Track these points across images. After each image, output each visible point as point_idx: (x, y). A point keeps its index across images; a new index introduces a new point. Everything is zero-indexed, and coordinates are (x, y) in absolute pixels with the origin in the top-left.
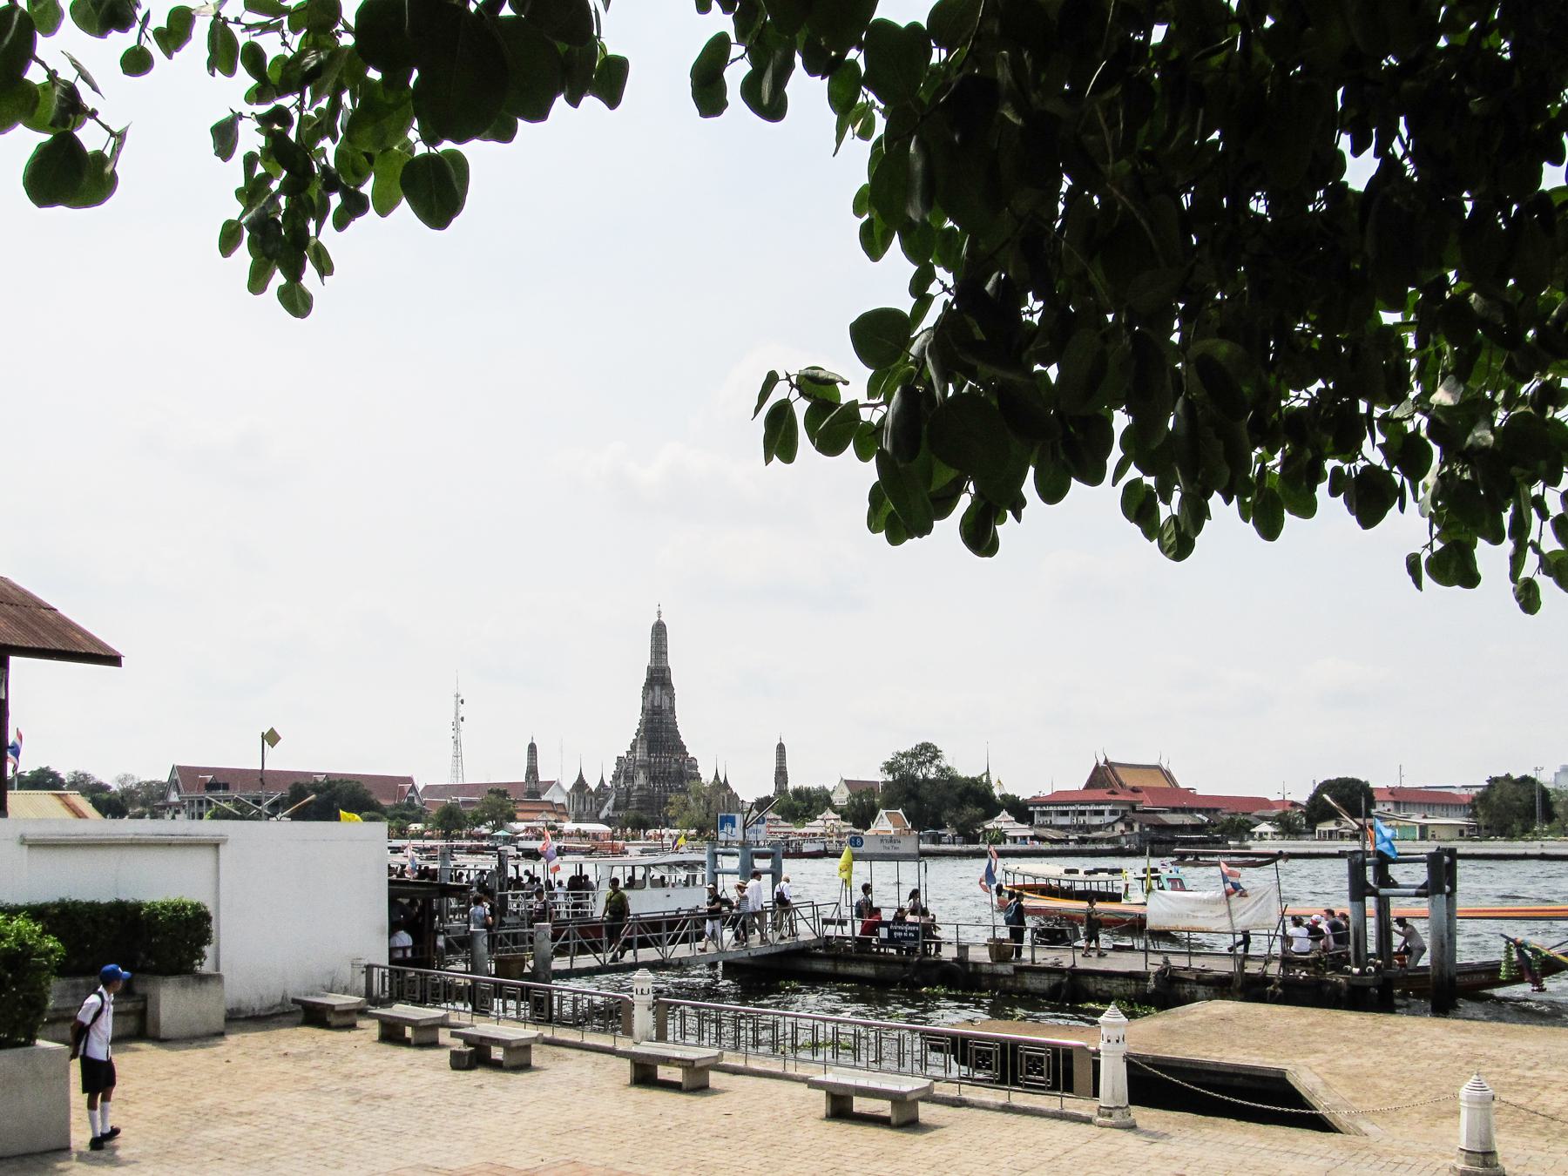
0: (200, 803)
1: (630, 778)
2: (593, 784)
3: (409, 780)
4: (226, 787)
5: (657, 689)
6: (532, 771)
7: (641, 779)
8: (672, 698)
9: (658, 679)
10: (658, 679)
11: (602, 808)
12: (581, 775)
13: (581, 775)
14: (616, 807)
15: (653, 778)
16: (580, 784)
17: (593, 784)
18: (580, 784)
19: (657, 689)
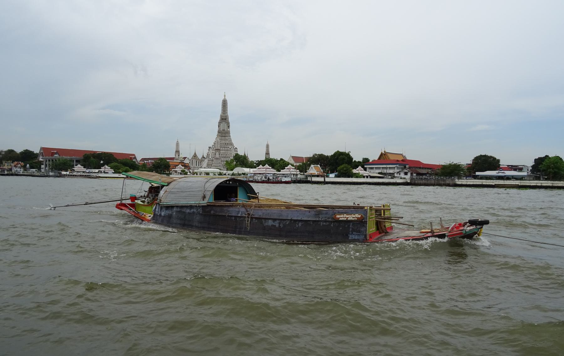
0: (49, 160)
2: (200, 157)
3: (134, 155)
6: (177, 152)
9: (224, 119)
10: (224, 119)
12: (195, 153)
13: (195, 153)
16: (195, 156)
17: (200, 157)
18: (195, 156)
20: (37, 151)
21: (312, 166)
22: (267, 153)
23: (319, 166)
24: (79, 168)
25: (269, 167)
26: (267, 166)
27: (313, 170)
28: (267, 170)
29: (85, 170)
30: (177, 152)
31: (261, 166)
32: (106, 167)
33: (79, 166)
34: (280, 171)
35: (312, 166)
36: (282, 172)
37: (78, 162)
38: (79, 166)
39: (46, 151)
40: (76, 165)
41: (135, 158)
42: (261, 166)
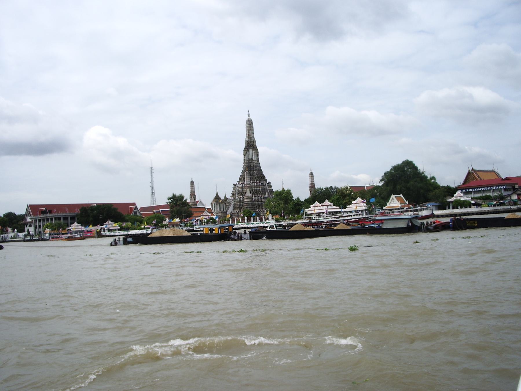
0: (40, 221)
1: (242, 193)
2: (222, 198)
3: (134, 204)
4: (50, 212)
5: (250, 150)
6: (193, 194)
7: (248, 194)
8: (258, 155)
9: (251, 146)
10: (251, 146)
11: (228, 209)
12: (217, 194)
13: (217, 194)
14: (235, 208)
15: (252, 193)
16: (217, 198)
17: (222, 198)
18: (217, 198)
19: (250, 150)
20: (20, 211)
21: (393, 196)
22: (312, 186)
23: (401, 195)
24: (75, 227)
25: (330, 203)
26: (327, 202)
27: (394, 202)
28: (329, 207)
29: (83, 228)
30: (193, 194)
31: (317, 203)
32: (110, 222)
33: (76, 224)
34: (345, 208)
35: (393, 196)
36: (349, 208)
37: (73, 219)
38: (76, 224)
39: (34, 209)
40: (72, 223)
41: (136, 208)
42: (317, 203)
